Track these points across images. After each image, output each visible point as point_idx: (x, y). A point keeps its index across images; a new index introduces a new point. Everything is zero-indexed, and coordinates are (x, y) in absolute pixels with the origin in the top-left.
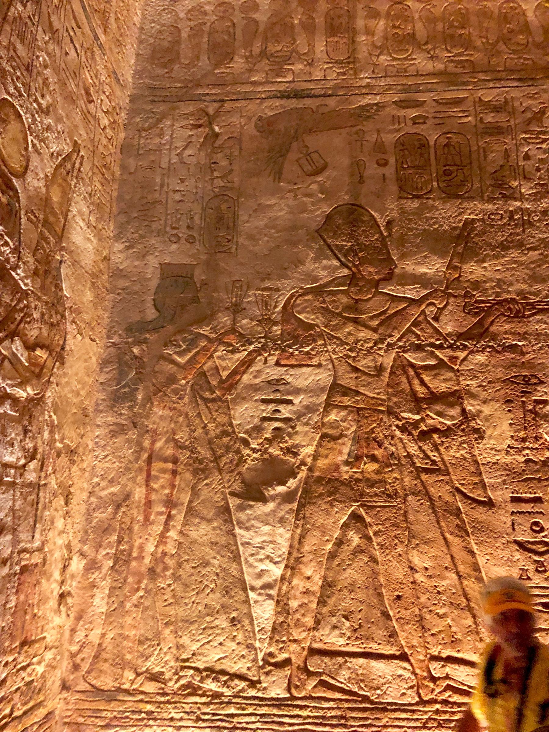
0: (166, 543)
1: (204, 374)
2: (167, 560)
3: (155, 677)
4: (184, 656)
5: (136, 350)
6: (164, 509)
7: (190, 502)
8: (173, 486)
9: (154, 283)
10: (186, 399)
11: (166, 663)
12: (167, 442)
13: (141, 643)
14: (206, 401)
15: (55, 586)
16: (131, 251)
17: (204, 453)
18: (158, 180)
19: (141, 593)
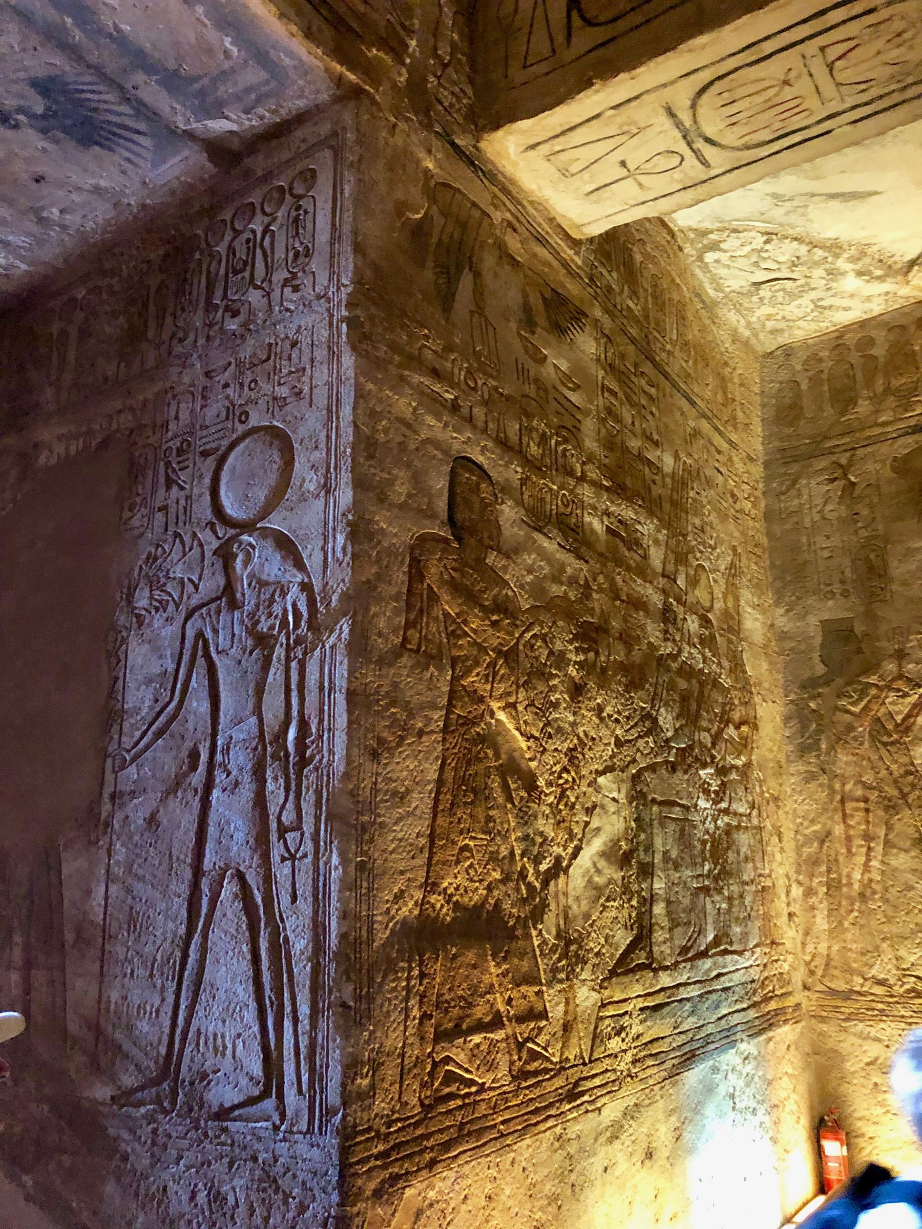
0: (870, 872)
1: (879, 719)
2: (874, 885)
3: (881, 983)
4: (904, 966)
5: (813, 705)
6: (863, 843)
7: (886, 835)
8: (868, 822)
9: (818, 640)
10: (866, 744)
11: (889, 971)
12: (855, 784)
13: (863, 954)
14: (885, 744)
15: (784, 905)
16: (791, 614)
17: (893, 792)
18: (804, 540)
19: (856, 914)
